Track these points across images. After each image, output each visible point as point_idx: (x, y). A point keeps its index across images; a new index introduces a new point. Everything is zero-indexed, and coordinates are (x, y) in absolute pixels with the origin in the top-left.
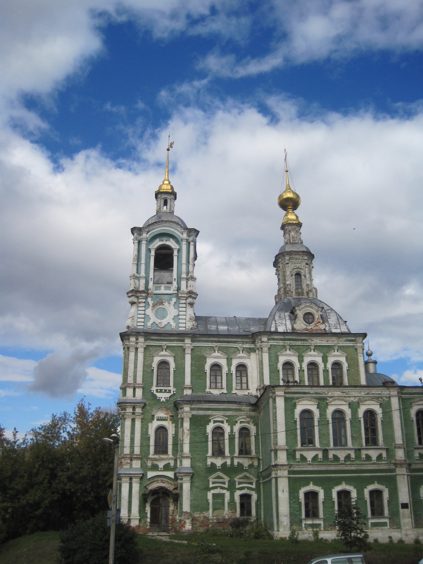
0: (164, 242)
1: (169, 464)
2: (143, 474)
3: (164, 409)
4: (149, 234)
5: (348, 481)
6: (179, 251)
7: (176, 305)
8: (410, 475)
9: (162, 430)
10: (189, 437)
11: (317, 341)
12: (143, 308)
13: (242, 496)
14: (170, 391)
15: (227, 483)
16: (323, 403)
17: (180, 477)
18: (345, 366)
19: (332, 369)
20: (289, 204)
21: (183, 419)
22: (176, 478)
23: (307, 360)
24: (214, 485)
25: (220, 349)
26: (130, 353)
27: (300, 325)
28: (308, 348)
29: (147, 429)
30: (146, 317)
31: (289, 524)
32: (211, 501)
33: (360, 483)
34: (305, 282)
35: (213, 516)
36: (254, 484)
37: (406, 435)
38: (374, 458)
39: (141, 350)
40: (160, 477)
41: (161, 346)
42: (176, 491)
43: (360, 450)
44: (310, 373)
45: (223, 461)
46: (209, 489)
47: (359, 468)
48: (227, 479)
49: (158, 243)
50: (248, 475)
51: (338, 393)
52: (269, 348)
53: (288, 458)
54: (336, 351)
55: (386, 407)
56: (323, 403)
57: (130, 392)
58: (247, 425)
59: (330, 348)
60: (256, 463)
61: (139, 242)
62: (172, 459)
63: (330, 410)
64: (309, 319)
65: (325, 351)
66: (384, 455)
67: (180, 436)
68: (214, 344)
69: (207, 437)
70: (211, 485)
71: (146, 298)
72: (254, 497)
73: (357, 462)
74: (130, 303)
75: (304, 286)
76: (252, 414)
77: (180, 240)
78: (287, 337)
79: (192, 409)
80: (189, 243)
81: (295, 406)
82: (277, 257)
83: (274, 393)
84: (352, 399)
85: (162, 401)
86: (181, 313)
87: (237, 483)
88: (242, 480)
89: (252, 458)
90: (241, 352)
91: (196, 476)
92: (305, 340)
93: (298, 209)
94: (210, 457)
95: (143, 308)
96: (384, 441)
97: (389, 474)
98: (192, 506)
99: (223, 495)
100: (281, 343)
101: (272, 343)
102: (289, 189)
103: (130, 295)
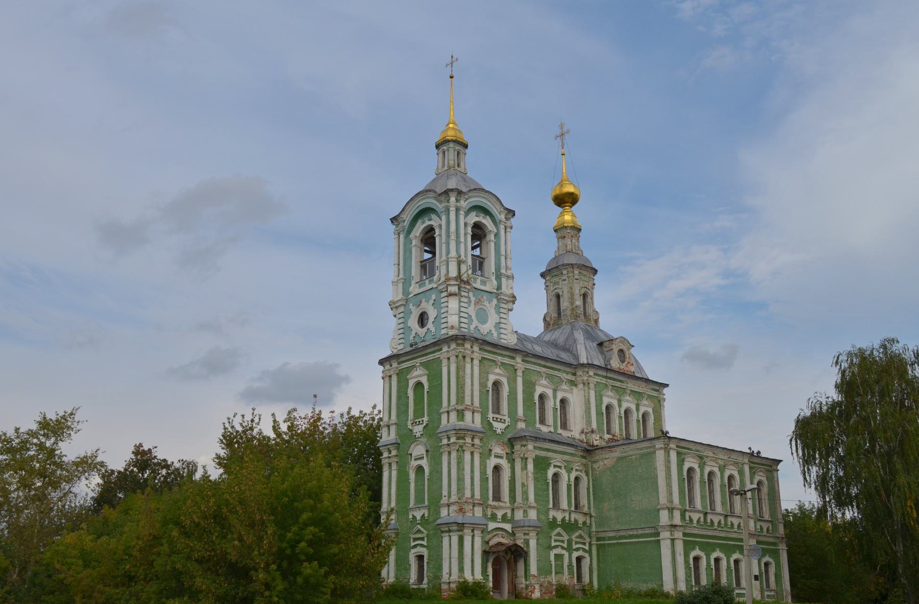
9: (497, 469)
11: (631, 385)
24: (558, 543)
29: (485, 467)
32: (553, 563)
39: (476, 362)
40: (500, 532)
41: (494, 361)
46: (551, 548)
48: (566, 538)
49: (473, 218)
55: (741, 473)
57: (468, 415)
60: (588, 521)
68: (544, 370)
70: (553, 544)
78: (609, 375)
79: (535, 448)
86: (502, 321)
88: (578, 540)
89: (585, 514)
98: (539, 569)
99: (563, 555)
100: (604, 381)
101: (598, 379)
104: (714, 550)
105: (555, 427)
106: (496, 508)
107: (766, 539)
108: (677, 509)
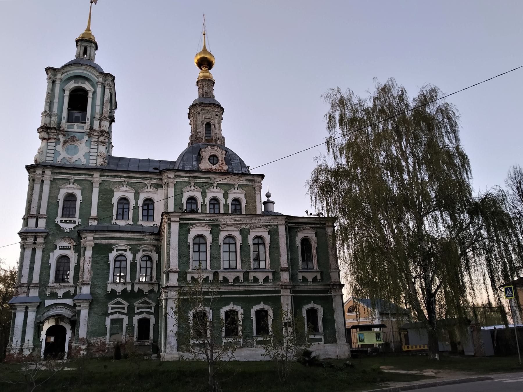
0: (80, 84)
1: (69, 291)
2: (40, 303)
3: (68, 239)
4: (63, 75)
5: (236, 301)
6: (94, 93)
7: (88, 143)
8: (294, 296)
10: (90, 265)
12: (54, 144)
13: (140, 321)
14: (75, 222)
15: (126, 308)
16: (215, 229)
17: (78, 304)
18: (244, 202)
19: (232, 204)
20: (205, 63)
21: (85, 248)
22: (75, 305)
23: (210, 195)
25: (128, 184)
26: (35, 185)
27: (205, 165)
28: (211, 184)
29: (48, 258)
30: (56, 153)
31: (176, 345)
32: (108, 327)
33: (247, 302)
34: (214, 131)
35: (110, 341)
36: (153, 308)
37: (291, 259)
38: (261, 280)
41: (69, 179)
42: (74, 318)
43: (248, 272)
44: (212, 207)
45: (124, 287)
46: (107, 314)
47: (247, 289)
48: (126, 304)
49: (72, 85)
50: (148, 300)
51: (231, 220)
52: (175, 184)
53: (178, 280)
54: (236, 189)
55: (274, 233)
56: (215, 229)
57: (32, 222)
58: (150, 253)
59: (232, 186)
60: (156, 289)
61: (54, 82)
62: (72, 286)
63: (222, 235)
64: (213, 160)
65: (227, 189)
66: (271, 277)
67: (81, 265)
69: (109, 265)
70: (110, 311)
71: (57, 135)
72: (153, 321)
73: (246, 284)
74: (40, 139)
75: (213, 134)
76: (156, 243)
77: (95, 83)
78: (192, 175)
79: (95, 238)
80: (104, 87)
81: (189, 231)
82: (191, 108)
83: (169, 219)
84: (243, 226)
85: (65, 231)
86: (92, 150)
87: (136, 308)
90: (149, 187)
91: (94, 302)
92: (209, 178)
93: (212, 69)
94: (111, 283)
95: (54, 144)
96: (270, 264)
97: (274, 295)
98: (88, 332)
99: (122, 320)
100: (187, 180)
102: (205, 50)
103: (40, 131)
104: (227, 304)
105: (135, 219)
106: (55, 288)
107: (311, 288)
108: (174, 272)
